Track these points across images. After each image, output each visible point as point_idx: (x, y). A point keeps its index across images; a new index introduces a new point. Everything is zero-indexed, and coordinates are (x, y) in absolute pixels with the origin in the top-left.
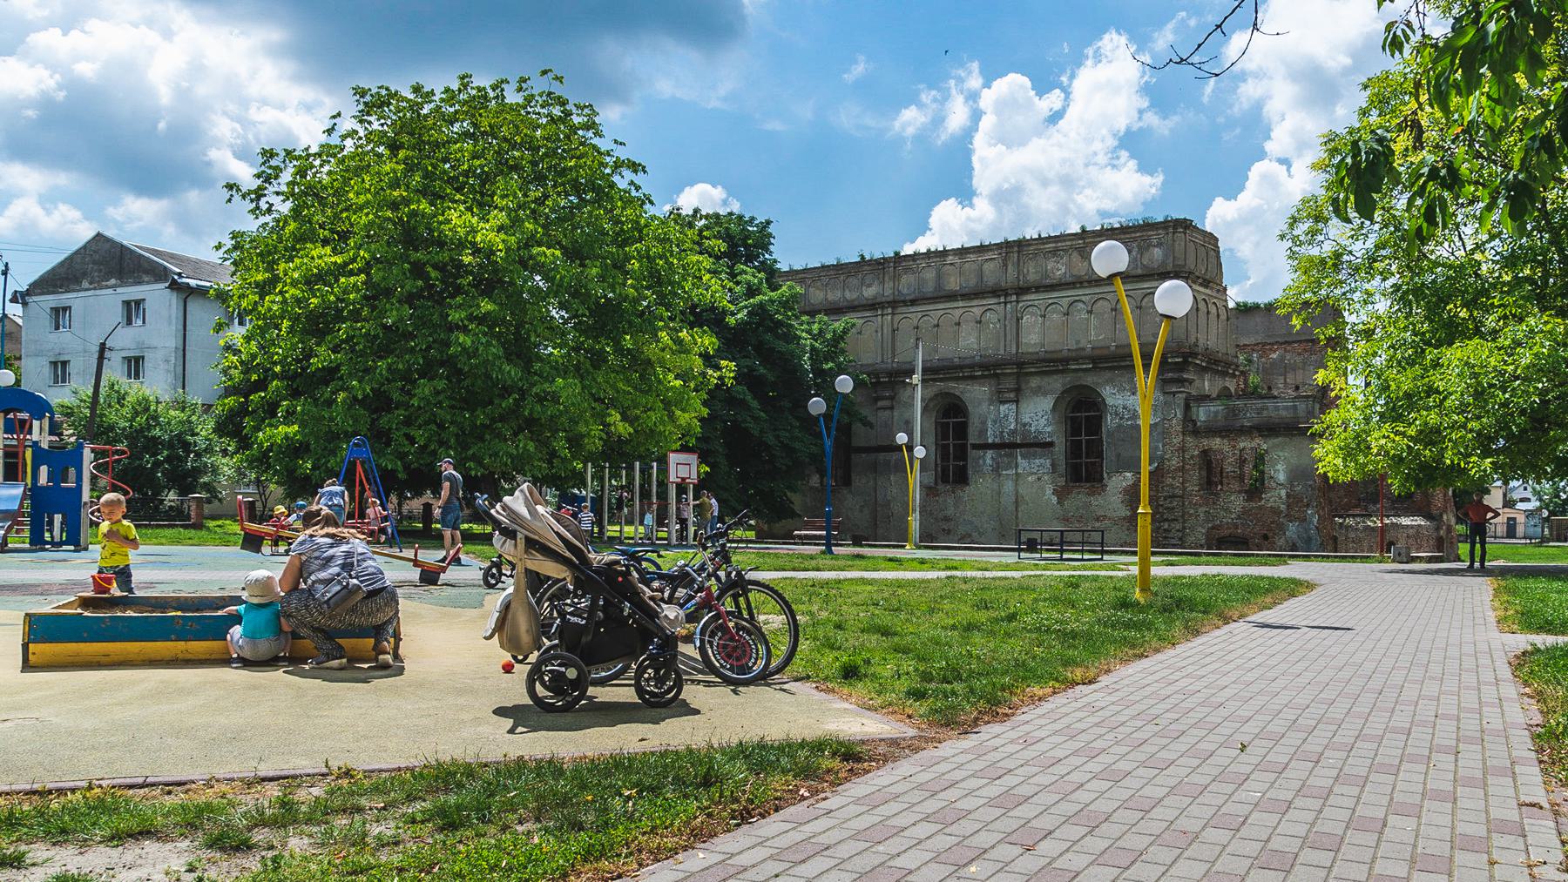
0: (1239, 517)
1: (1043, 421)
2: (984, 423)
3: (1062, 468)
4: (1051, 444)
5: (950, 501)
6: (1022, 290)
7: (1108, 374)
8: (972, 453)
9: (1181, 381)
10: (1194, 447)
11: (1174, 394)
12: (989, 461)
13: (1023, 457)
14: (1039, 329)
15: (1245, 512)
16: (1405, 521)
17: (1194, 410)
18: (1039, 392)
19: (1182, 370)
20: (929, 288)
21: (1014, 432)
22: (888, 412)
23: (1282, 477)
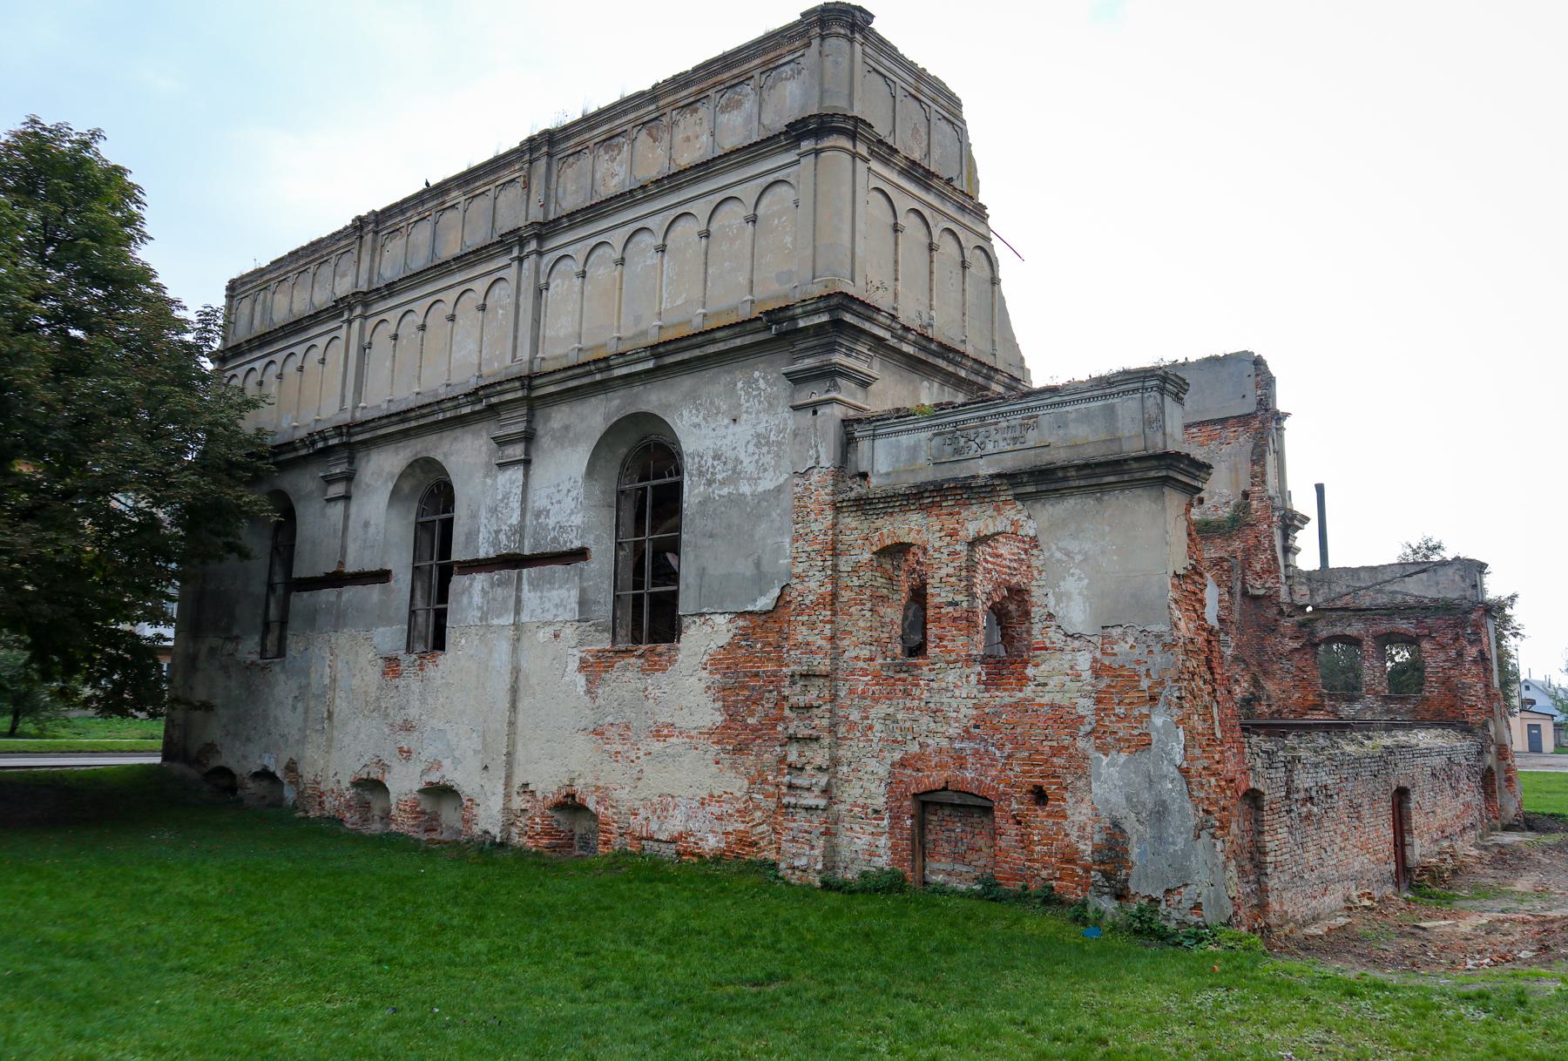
0: (967, 735)
1: (569, 503)
2: (474, 516)
3: (603, 610)
4: (581, 554)
5: (416, 686)
6: (545, 230)
7: (686, 382)
8: (458, 582)
9: (829, 374)
10: (862, 538)
11: (814, 407)
12: (477, 599)
13: (534, 586)
14: (594, 304)
15: (983, 720)
16: (1424, 738)
17: (864, 446)
18: (566, 437)
19: (831, 348)
20: (418, 263)
21: (520, 530)
22: (340, 506)
23: (1077, 615)
